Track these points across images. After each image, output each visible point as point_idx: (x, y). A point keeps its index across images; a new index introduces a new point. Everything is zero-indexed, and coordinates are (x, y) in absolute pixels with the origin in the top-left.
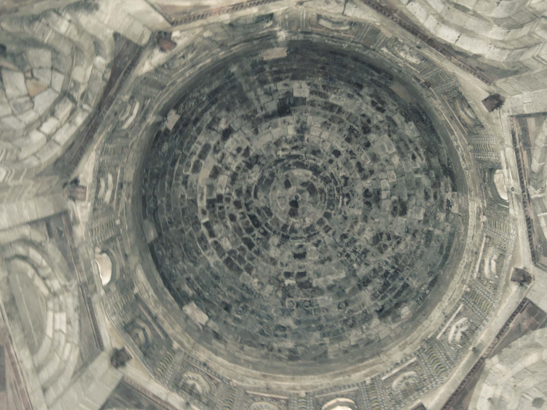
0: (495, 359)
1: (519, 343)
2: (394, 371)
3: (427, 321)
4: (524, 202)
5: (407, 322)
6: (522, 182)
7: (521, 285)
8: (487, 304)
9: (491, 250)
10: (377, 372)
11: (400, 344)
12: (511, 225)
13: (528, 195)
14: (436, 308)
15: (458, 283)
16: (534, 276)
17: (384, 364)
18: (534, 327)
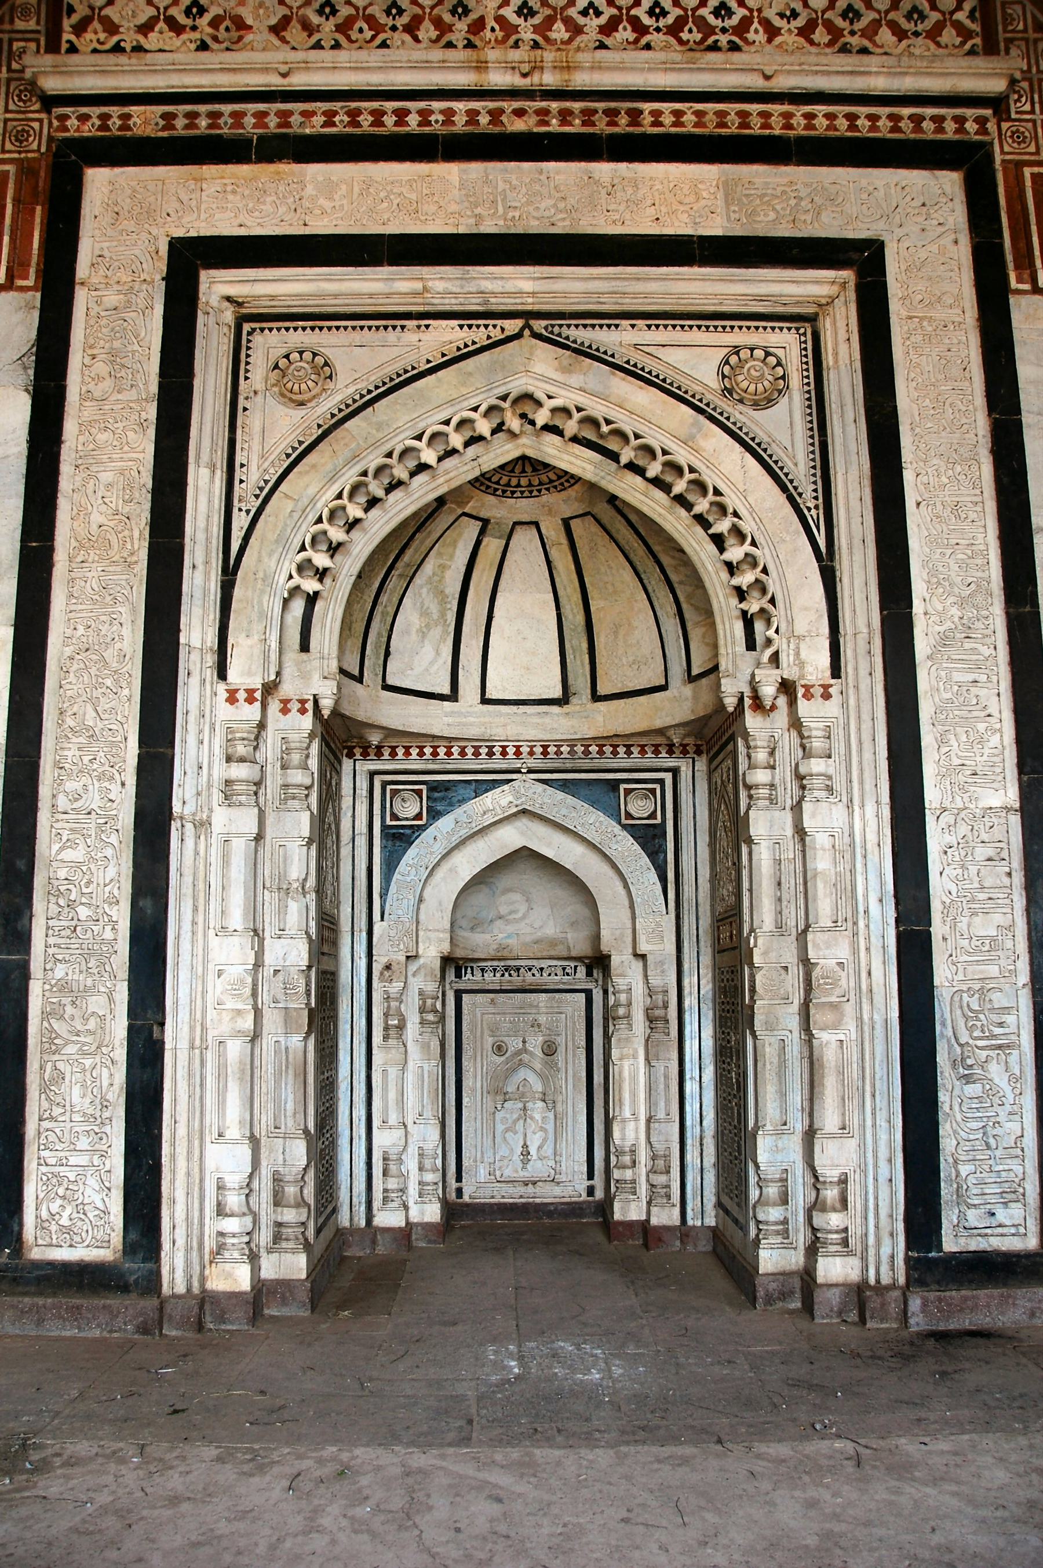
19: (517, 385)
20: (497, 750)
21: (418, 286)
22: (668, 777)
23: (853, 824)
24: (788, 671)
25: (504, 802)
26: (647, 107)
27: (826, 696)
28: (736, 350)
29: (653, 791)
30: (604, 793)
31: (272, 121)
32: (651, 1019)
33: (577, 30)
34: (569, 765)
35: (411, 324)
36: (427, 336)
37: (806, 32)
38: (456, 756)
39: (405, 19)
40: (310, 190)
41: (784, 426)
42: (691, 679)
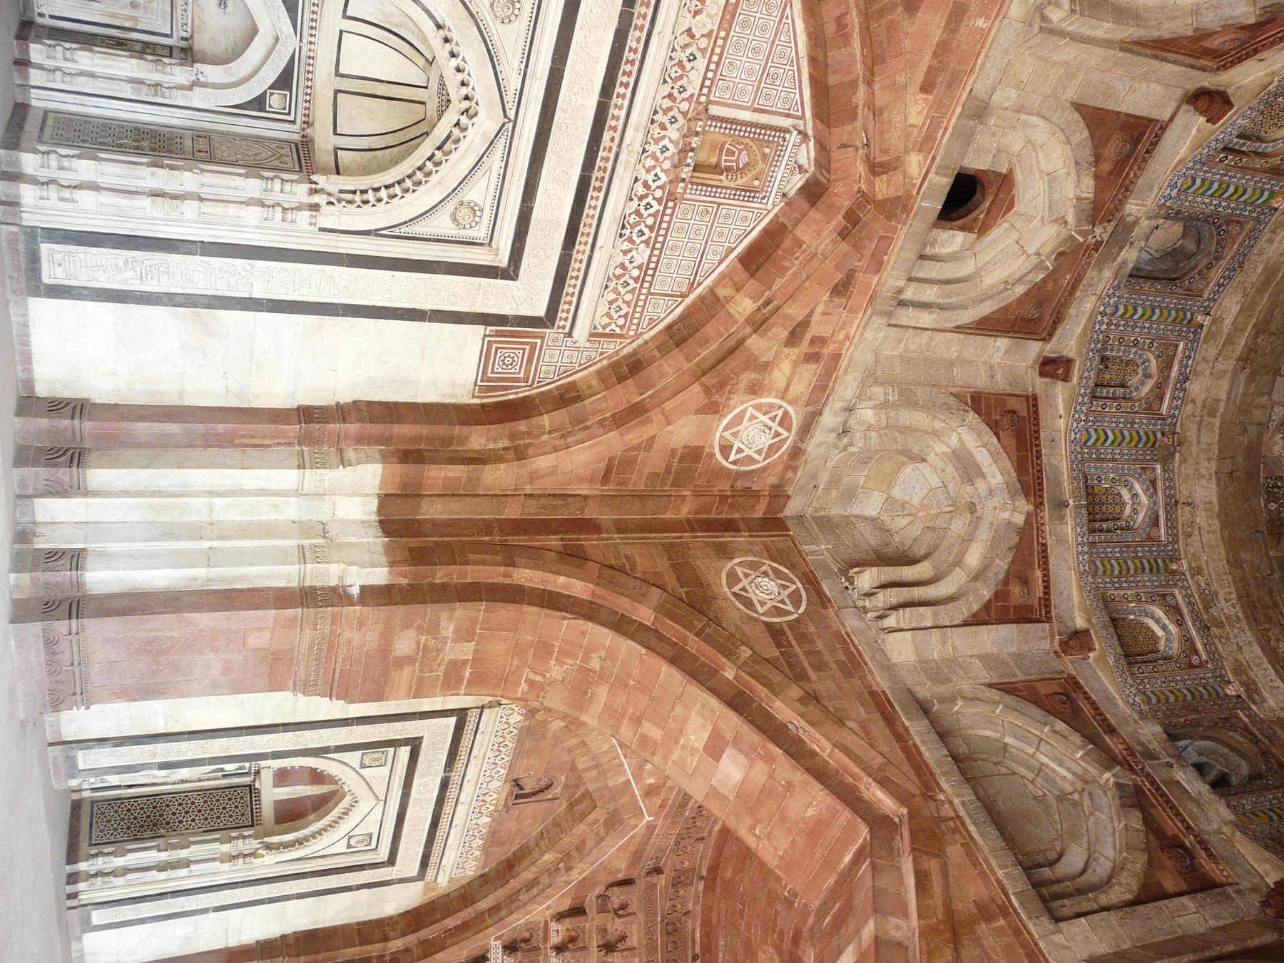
0: (1019, 519)
1: (1002, 565)
2: (1176, 367)
3: (1212, 471)
4: (1133, 755)
5: (1260, 436)
6: (1153, 782)
7: (1076, 634)
9: (1175, 648)
11: (1222, 404)
12: (1145, 708)
13: (1132, 770)
14: (1215, 500)
16: (1059, 657)
17: (1212, 359)
20: (313, 32)
22: (291, 118)
23: (251, 227)
24: (325, 209)
25: (284, 29)
26: (602, 195)
27: (311, 224)
28: (481, 210)
30: (284, 81)
31: (639, 22)
33: (648, 171)
34: (302, 69)
35: (523, 66)
36: (515, 73)
37: (622, 266)
39: (676, 94)
40: (600, 33)
41: (441, 224)
42: (336, 149)
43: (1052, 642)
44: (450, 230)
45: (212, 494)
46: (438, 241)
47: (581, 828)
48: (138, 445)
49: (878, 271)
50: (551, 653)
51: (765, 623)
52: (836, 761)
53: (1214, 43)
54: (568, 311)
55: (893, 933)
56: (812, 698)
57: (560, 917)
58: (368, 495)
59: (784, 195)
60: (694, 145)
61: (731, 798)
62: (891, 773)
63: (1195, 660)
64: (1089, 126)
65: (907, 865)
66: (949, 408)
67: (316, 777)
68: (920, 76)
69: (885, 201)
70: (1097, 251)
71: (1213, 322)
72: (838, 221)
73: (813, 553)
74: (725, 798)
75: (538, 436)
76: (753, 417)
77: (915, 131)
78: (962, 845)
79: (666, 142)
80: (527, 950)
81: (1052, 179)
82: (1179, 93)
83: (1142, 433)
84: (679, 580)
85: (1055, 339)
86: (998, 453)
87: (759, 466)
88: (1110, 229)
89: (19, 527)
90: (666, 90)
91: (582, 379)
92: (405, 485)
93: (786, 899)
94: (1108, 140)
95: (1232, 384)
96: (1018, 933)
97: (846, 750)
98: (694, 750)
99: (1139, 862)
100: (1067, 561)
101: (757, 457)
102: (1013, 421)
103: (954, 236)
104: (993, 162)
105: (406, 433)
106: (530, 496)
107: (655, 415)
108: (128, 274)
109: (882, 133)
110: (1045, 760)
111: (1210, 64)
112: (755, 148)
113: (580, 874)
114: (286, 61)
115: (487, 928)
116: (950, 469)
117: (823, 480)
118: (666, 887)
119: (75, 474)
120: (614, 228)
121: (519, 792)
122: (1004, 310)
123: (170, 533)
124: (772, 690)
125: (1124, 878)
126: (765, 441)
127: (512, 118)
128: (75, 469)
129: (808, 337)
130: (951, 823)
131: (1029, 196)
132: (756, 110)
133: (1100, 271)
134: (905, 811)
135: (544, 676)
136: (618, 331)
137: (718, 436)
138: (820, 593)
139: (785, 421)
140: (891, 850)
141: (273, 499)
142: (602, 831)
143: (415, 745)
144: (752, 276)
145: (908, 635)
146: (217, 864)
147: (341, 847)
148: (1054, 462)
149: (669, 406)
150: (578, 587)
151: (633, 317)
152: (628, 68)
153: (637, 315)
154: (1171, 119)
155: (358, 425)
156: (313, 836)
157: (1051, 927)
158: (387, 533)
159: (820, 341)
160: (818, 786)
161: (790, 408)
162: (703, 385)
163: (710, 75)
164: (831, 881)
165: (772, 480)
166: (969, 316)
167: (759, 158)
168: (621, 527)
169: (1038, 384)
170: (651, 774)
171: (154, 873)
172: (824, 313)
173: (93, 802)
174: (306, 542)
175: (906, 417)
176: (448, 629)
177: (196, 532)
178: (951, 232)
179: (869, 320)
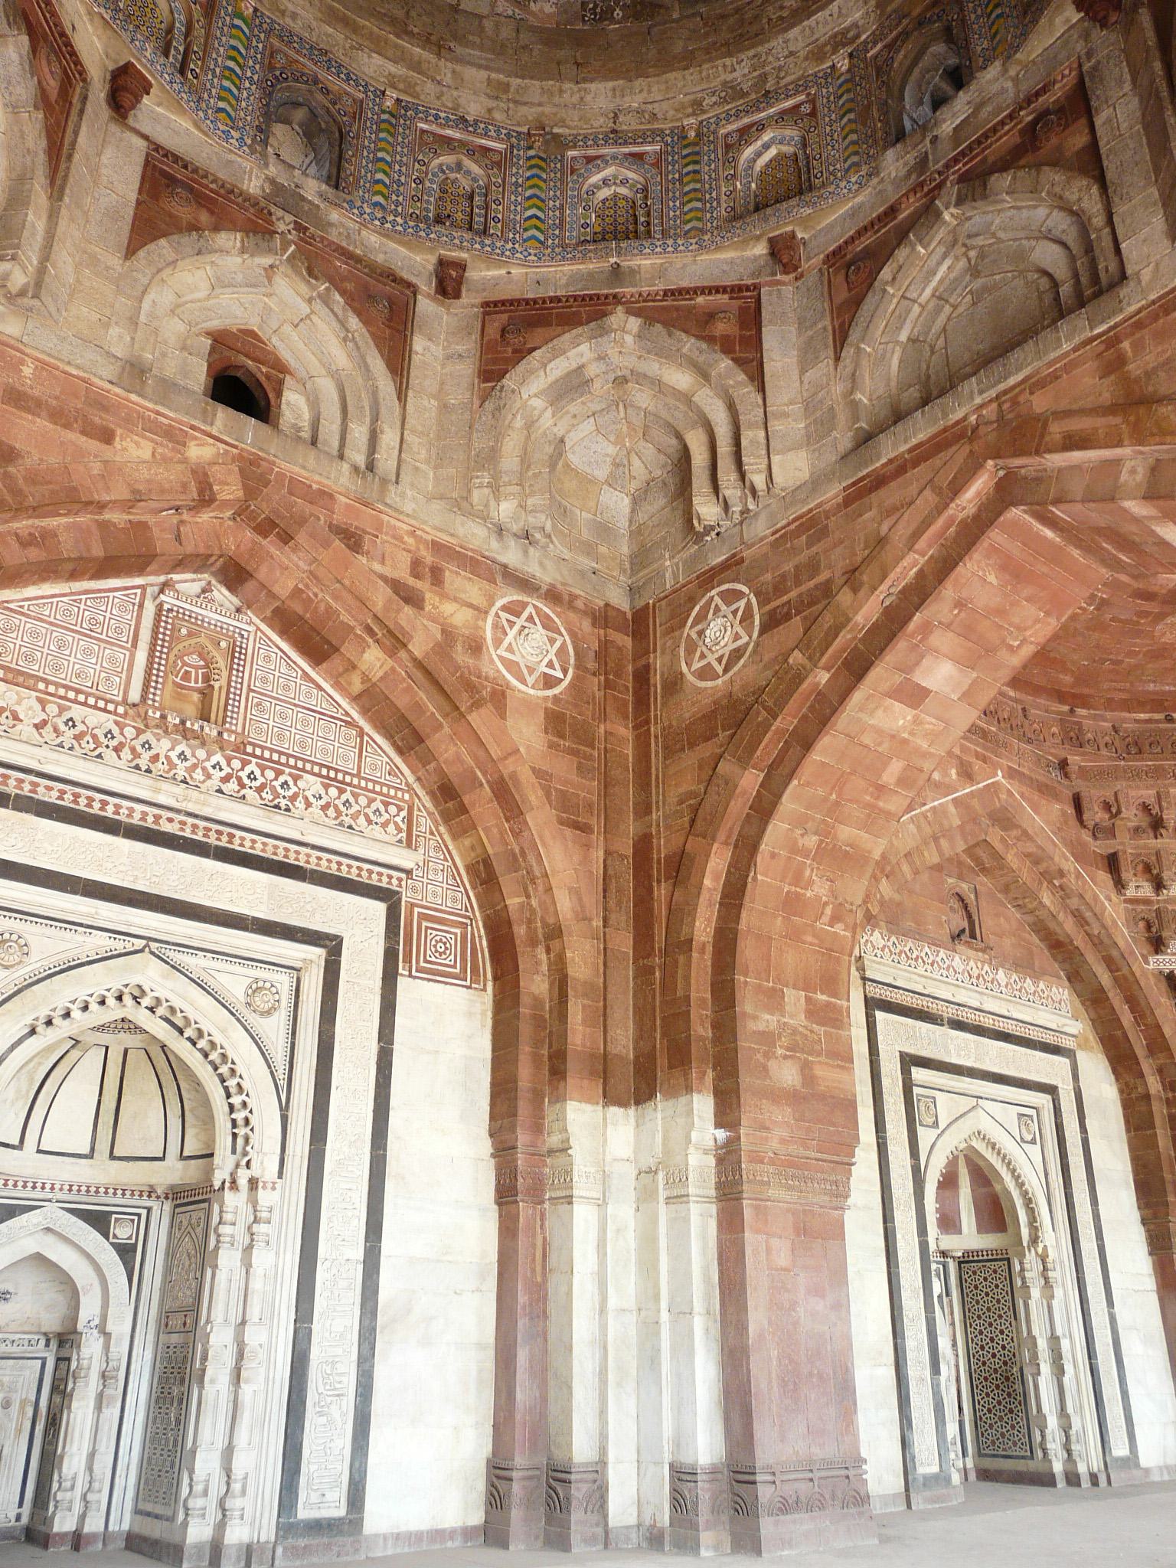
0: (634, 323)
1: (689, 345)
2: (449, 132)
3: (575, 88)
4: (921, 185)
5: (533, 29)
6: (955, 160)
8: (699, 215)
9: (792, 133)
10: (417, 97)
11: (493, 75)
13: (939, 186)
14: (611, 84)
15: (686, 95)
16: (802, 275)
17: (438, 88)
18: (727, 348)
19: (134, 980)
20: (39, 1185)
21: (93, 911)
22: (144, 1212)
24: (255, 1171)
25: (35, 1221)
26: (238, 833)
27: (274, 1188)
28: (257, 980)
29: (133, 1221)
30: (99, 1221)
31: (27, 787)
32: (104, 1376)
33: (209, 776)
34: (84, 1199)
36: (89, 939)
37: (325, 808)
38: (10, 1186)
39: (115, 743)
40: (40, 836)
41: (274, 1030)
42: (182, 1158)
43: (783, 283)
44: (282, 1017)
45: (603, 1310)
46: (294, 1033)
47: (1011, 859)
48: (544, 1399)
49: (331, 497)
50: (797, 894)
51: (761, 634)
52: (930, 546)
53: (53, 85)
54: (380, 874)
55: (1139, 477)
56: (852, 577)
57: (1120, 885)
58: (605, 1119)
59: (238, 610)
60: (177, 721)
61: (974, 675)
62: (945, 479)
63: (806, 109)
64: (155, 238)
65: (1057, 460)
66: (499, 409)
67: (949, 1182)
68: (93, 445)
69: (245, 487)
70: (306, 229)
71: (393, 86)
72: (270, 545)
73: (675, 575)
74: (975, 682)
75: (533, 911)
76: (510, 649)
77: (160, 450)
78: (1032, 393)
79: (173, 755)
80: (1161, 924)
81: (219, 283)
82: (114, 128)
83: (528, 174)
84: (708, 739)
85: (414, 280)
86: (553, 349)
87: (569, 642)
88: (280, 213)
89: (644, 1545)
90: (109, 755)
91: (462, 856)
92: (593, 1073)
93: (1097, 609)
94: (171, 215)
95: (469, 63)
96: (1139, 326)
97: (916, 535)
98: (916, 721)
99: (1053, 177)
100: (685, 266)
101: (558, 644)
102: (515, 331)
103: (288, 403)
104: (197, 356)
105: (528, 1073)
106: (605, 920)
107: (508, 768)
108: (335, 1411)
109: (163, 491)
110: (928, 292)
111: (78, 90)
112: (180, 646)
113: (1067, 860)
114: (74, 1219)
115: (1133, 974)
116: (573, 408)
117: (586, 563)
118: (1082, 754)
119: (579, 1476)
120: (279, 818)
121: (968, 934)
122: (378, 341)
123: (650, 1360)
124: (842, 626)
125: (1072, 195)
126: (539, 634)
127: (144, 942)
128: (573, 1477)
129: (411, 581)
130: (1006, 406)
131: (239, 312)
132: (135, 645)
133: (330, 224)
134: (990, 462)
135: (826, 904)
136: (404, 814)
137: (532, 692)
138: (725, 566)
139: (514, 609)
140: (1038, 480)
141: (610, 1235)
142: (1015, 833)
143: (909, 1061)
144: (337, 650)
145: (776, 459)
146: (1055, 1303)
147: (1035, 1151)
148: (563, 281)
149: (495, 752)
150: (717, 864)
151: (388, 796)
152: (83, 801)
153: (385, 790)
154: (146, 137)
155: (519, 1130)
156: (1021, 1185)
157: (1132, 284)
158: (651, 1096)
159: (416, 567)
160: (960, 568)
161: (499, 604)
162: (471, 709)
163: (91, 701)
164: (1076, 553)
165: (586, 624)
166: (386, 385)
167: (193, 641)
168: (644, 809)
169: (469, 301)
170: (946, 774)
171: (1066, 1380)
172: (383, 563)
173: (979, 1454)
174: (662, 1195)
175: (509, 461)
176: (767, 1021)
177: (649, 1329)
178: (283, 406)
179: (390, 507)
